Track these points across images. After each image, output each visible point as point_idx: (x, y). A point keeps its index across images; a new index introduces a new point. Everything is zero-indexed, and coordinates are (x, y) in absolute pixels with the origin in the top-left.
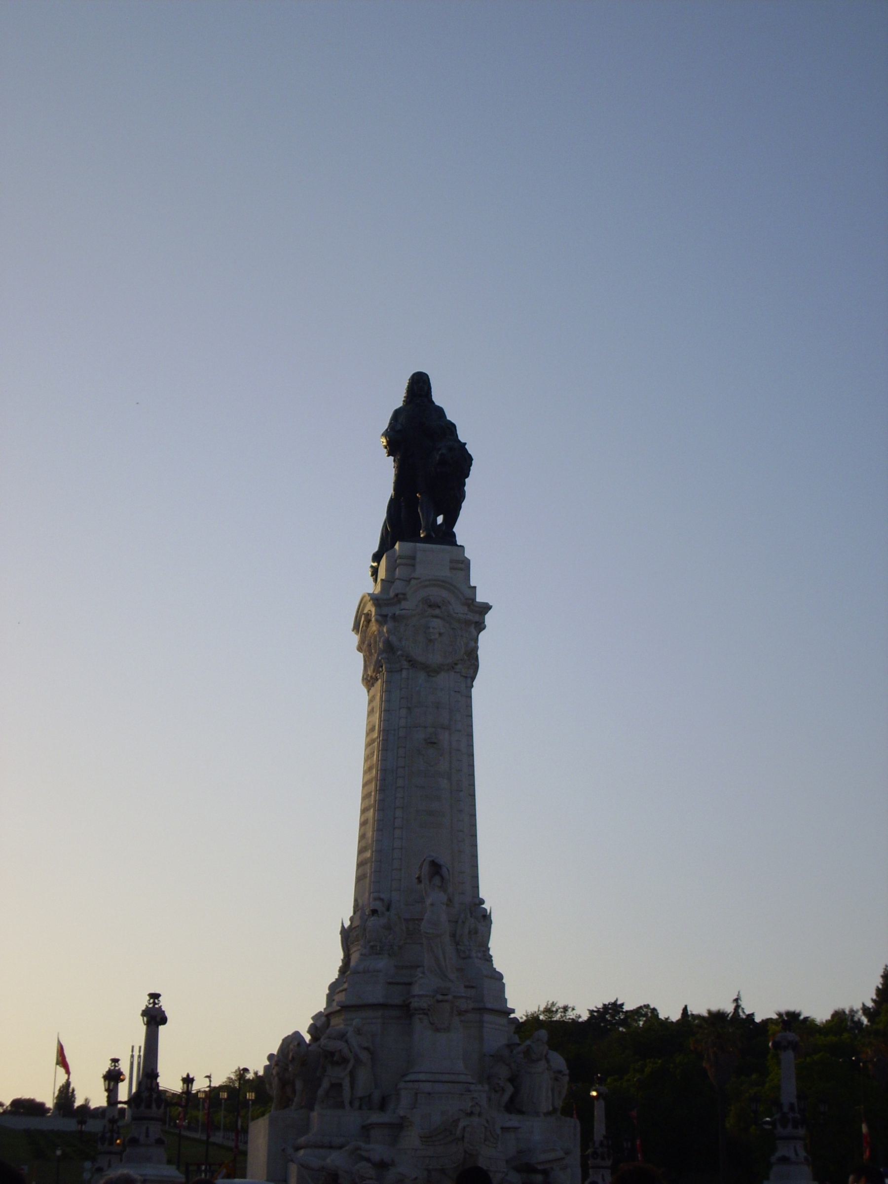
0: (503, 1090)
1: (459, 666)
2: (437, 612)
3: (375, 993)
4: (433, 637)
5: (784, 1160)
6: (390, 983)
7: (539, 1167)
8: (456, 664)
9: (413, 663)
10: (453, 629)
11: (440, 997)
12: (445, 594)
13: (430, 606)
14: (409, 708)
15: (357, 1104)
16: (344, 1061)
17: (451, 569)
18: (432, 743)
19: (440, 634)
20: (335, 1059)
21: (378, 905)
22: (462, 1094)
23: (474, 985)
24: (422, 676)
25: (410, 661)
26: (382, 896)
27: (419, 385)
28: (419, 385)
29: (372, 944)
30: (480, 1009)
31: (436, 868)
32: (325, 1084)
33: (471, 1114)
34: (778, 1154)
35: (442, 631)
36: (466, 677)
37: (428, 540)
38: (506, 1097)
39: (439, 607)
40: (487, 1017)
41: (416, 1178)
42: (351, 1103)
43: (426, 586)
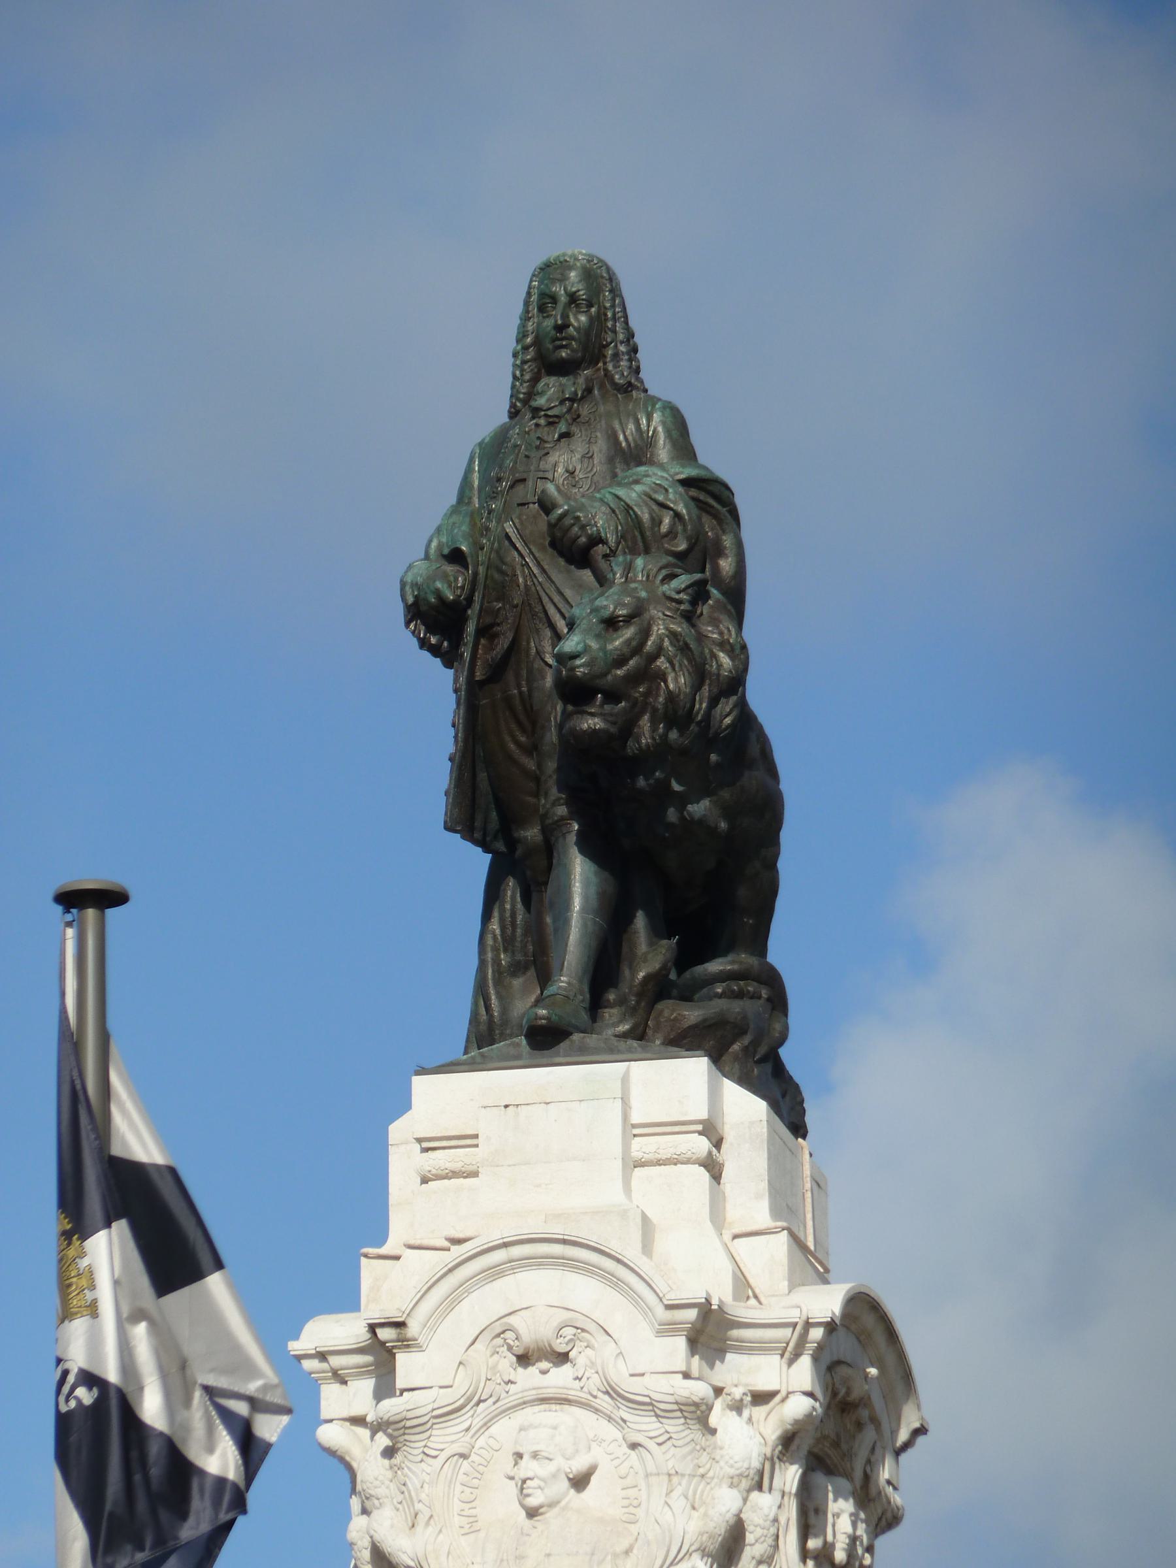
2: (559, 1378)
10: (634, 1446)
12: (584, 1293)
13: (524, 1359)
35: (578, 1465)
43: (494, 1273)
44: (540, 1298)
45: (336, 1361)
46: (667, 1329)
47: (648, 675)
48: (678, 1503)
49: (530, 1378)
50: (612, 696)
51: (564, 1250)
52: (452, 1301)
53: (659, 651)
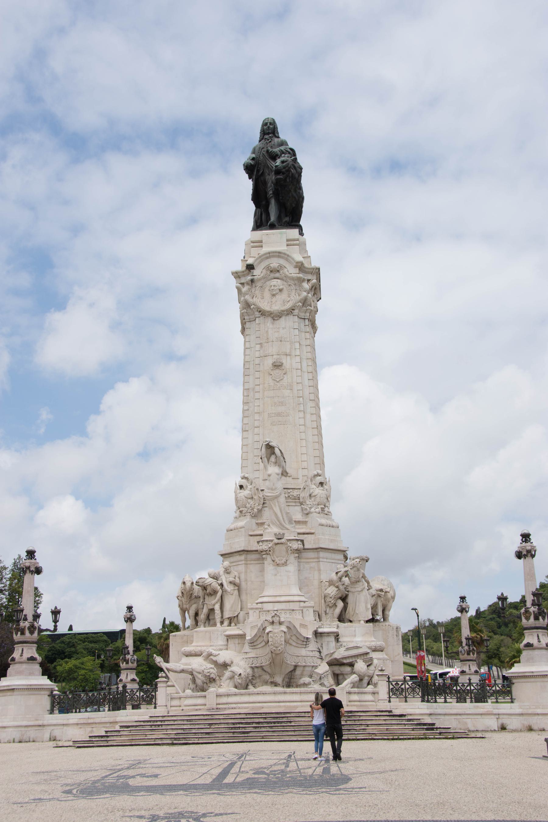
0: (335, 605)
1: (296, 312)
2: (277, 275)
3: (240, 543)
4: (274, 293)
5: (529, 646)
6: (251, 536)
7: (345, 661)
8: (293, 310)
9: (263, 313)
10: (290, 285)
11: (276, 541)
12: (282, 262)
13: (271, 271)
14: (261, 344)
15: (226, 623)
16: (215, 592)
17: (287, 245)
18: (277, 366)
19: (281, 290)
20: (208, 591)
21: (244, 482)
22: (293, 610)
23: (312, 531)
24: (269, 320)
25: (260, 311)
26: (246, 475)
27: (269, 130)
28: (269, 130)
29: (241, 509)
30: (316, 549)
31: (270, 448)
32: (205, 611)
33: (273, 623)
34: (525, 642)
35: (281, 287)
36: (304, 319)
37: (272, 227)
38: (338, 611)
39: (278, 271)
40: (322, 554)
41: (240, 674)
42: (222, 623)
43: (267, 258)
44: (274, 263)
45: (239, 274)
46: (296, 267)
47: (289, 171)
48: (297, 295)
49: (272, 275)
50: (283, 173)
51: (279, 254)
52: (260, 262)
53: (291, 167)
